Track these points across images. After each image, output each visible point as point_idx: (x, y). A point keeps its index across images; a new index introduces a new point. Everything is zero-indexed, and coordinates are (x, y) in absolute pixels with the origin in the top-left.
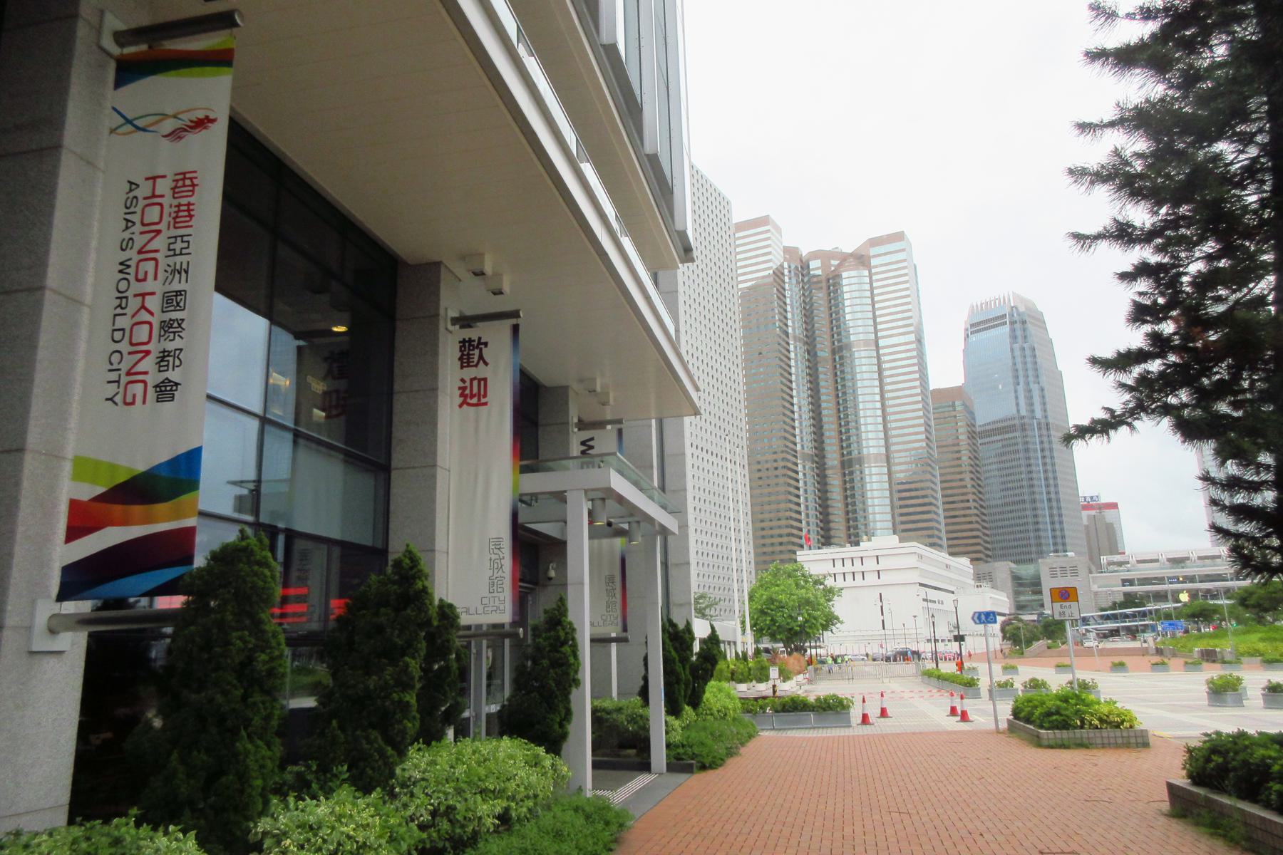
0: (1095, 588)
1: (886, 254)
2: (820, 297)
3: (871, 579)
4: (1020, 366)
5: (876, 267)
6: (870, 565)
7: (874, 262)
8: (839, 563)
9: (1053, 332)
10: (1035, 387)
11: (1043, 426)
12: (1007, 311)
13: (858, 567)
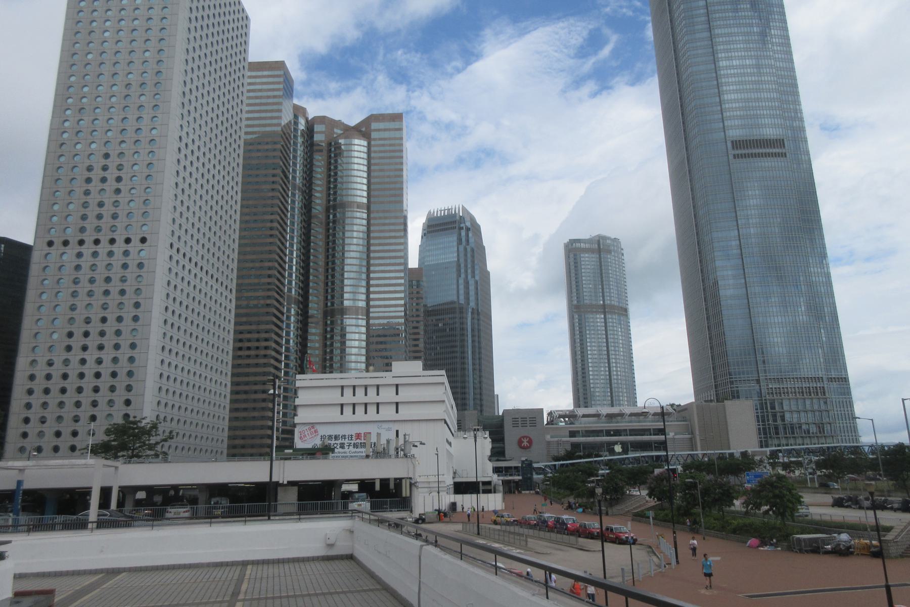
0: (548, 438)
1: (385, 130)
2: (320, 161)
3: (388, 412)
4: (462, 260)
5: (375, 139)
6: (387, 395)
7: (374, 135)
8: (348, 392)
9: (485, 243)
10: (472, 282)
11: (476, 311)
12: (458, 218)
13: (372, 396)
